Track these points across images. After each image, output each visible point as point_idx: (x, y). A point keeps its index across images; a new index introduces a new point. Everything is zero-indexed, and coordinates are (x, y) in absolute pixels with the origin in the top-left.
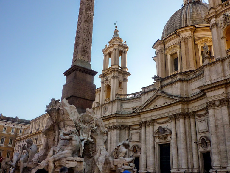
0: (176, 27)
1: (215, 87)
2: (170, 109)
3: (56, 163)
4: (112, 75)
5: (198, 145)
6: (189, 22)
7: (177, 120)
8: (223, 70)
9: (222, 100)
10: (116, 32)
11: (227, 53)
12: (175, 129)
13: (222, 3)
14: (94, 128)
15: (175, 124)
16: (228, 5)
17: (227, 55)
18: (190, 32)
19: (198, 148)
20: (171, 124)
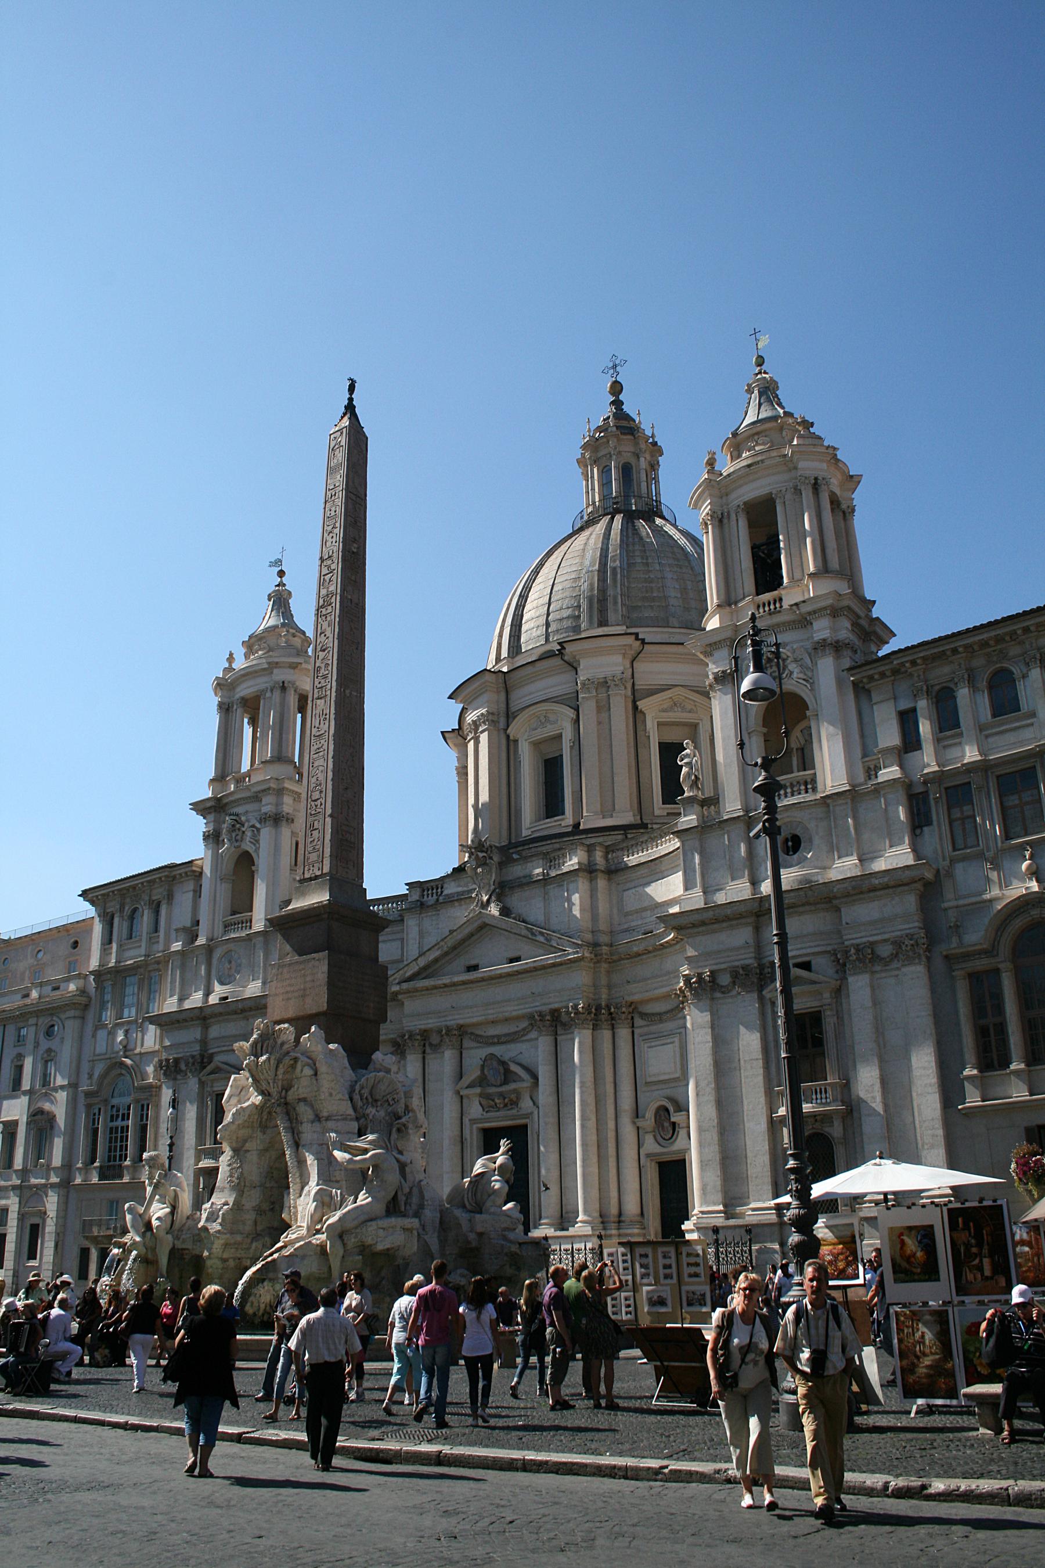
1: (717, 921)
3: (345, 1237)
4: (264, 809)
6: (616, 611)
9: (741, 972)
10: (281, 600)
12: (552, 1068)
13: (758, 594)
14: (403, 1120)
15: (553, 1049)
16: (779, 612)
18: (618, 659)
20: (537, 1048)
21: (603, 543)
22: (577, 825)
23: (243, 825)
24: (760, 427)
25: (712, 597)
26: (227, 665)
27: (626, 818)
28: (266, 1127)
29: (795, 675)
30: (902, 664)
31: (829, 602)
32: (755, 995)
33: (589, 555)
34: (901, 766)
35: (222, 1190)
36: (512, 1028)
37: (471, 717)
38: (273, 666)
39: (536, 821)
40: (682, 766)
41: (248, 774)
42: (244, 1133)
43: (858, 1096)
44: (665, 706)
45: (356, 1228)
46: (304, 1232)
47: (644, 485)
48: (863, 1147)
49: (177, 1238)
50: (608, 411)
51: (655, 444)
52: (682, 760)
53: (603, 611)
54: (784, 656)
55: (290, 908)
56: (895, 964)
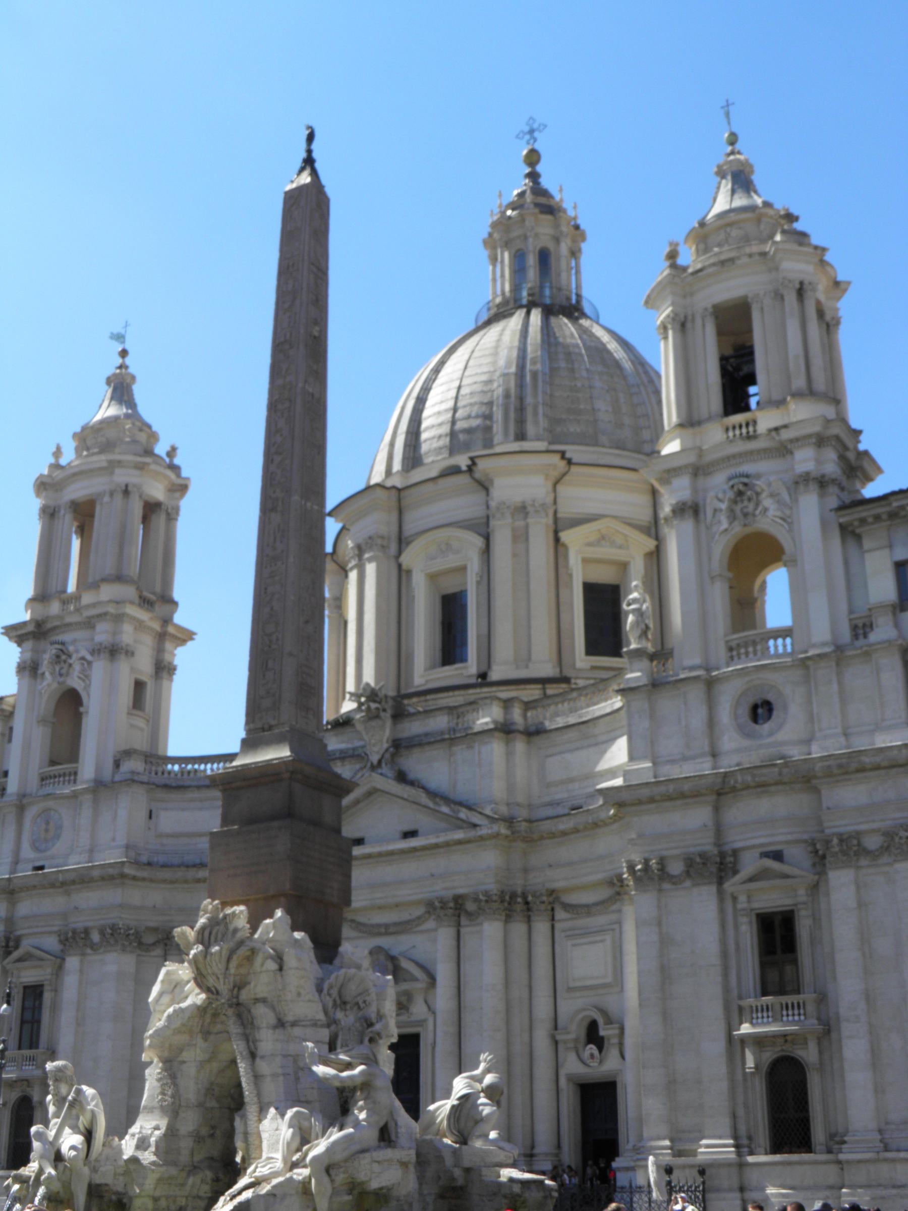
0: (468, 431)
2: (438, 863)
3: (332, 1172)
5: (561, 1048)
6: (536, 423)
7: (464, 921)
8: (712, 723)
9: (698, 860)
11: (731, 649)
12: (452, 966)
15: (455, 943)
17: (732, 658)
19: (560, 1060)
21: (520, 341)
22: (483, 676)
23: (70, 656)
24: (733, 217)
25: (670, 414)
26: (52, 460)
27: (548, 670)
29: (771, 513)
31: (817, 428)
32: (713, 888)
33: (503, 354)
34: (897, 625)
35: (150, 1110)
36: (404, 916)
38: (113, 465)
40: (627, 613)
41: (77, 597)
42: (184, 1038)
45: (346, 1160)
46: (279, 1165)
47: (564, 276)
48: (842, 1076)
49: (94, 1170)
50: (523, 184)
51: (577, 227)
52: (629, 604)
53: (521, 422)
54: (758, 489)
55: (235, 764)
56: (885, 859)
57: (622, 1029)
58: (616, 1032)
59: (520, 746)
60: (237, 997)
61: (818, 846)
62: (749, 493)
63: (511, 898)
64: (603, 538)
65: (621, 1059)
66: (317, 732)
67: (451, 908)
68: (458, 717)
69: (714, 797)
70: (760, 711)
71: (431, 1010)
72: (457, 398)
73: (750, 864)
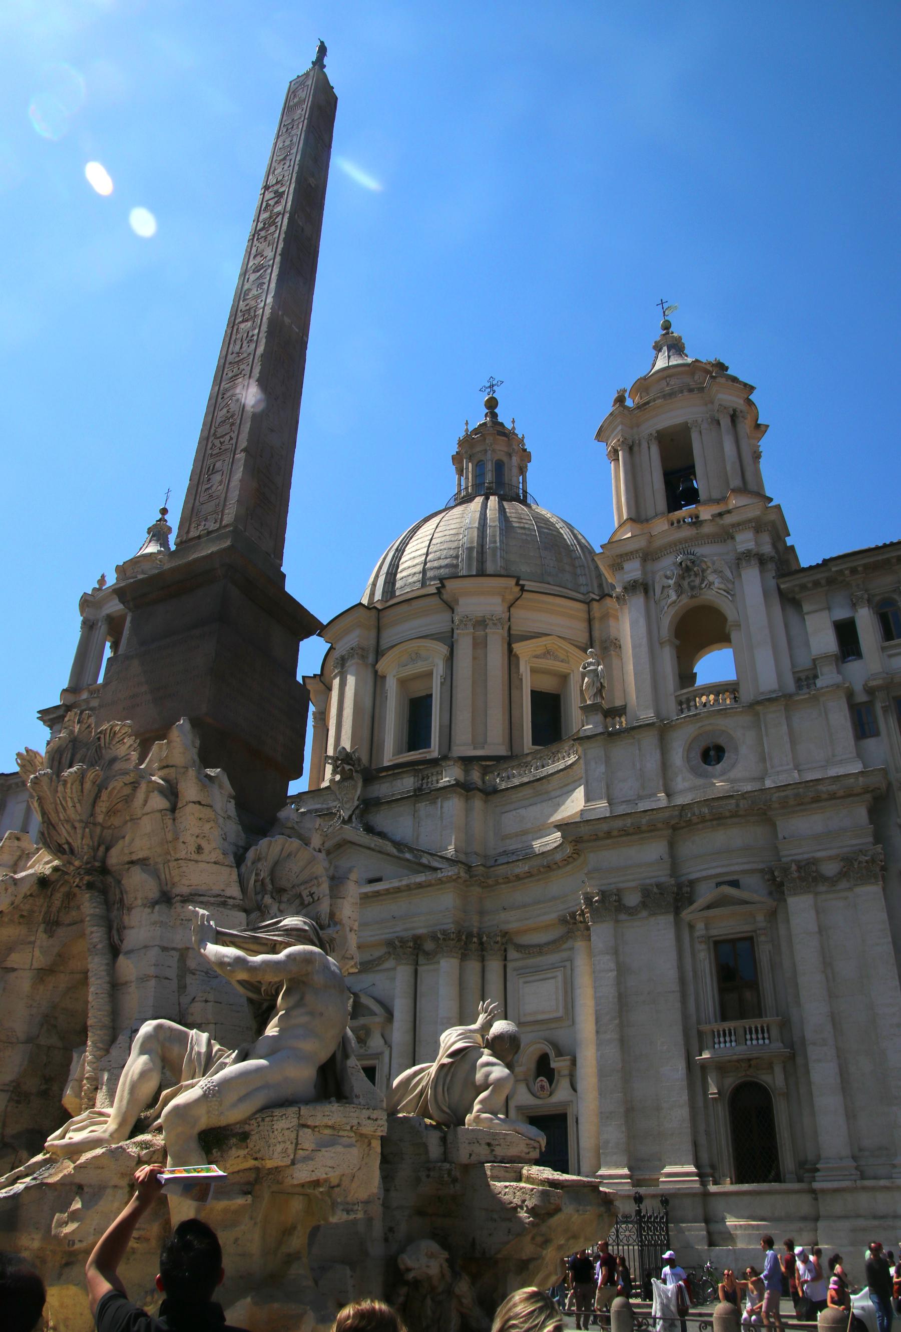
7: (421, 960)
8: (665, 766)
9: (655, 890)
11: (680, 703)
15: (412, 980)
18: (498, 600)
27: (502, 751)
28: (57, 923)
29: (716, 585)
30: (841, 572)
32: (671, 918)
34: (839, 672)
37: (342, 648)
39: (398, 754)
43: (803, 1039)
44: (538, 653)
51: (525, 450)
54: (704, 567)
56: (844, 884)
57: (574, 1062)
58: (568, 1063)
59: (478, 803)
60: (104, 861)
61: (776, 874)
62: (695, 569)
63: (467, 938)
64: (547, 654)
65: (573, 1092)
66: (273, 556)
67: (410, 947)
68: (423, 779)
69: (670, 831)
70: (712, 753)
71: (388, 1043)
72: (429, 546)
73: (706, 894)
